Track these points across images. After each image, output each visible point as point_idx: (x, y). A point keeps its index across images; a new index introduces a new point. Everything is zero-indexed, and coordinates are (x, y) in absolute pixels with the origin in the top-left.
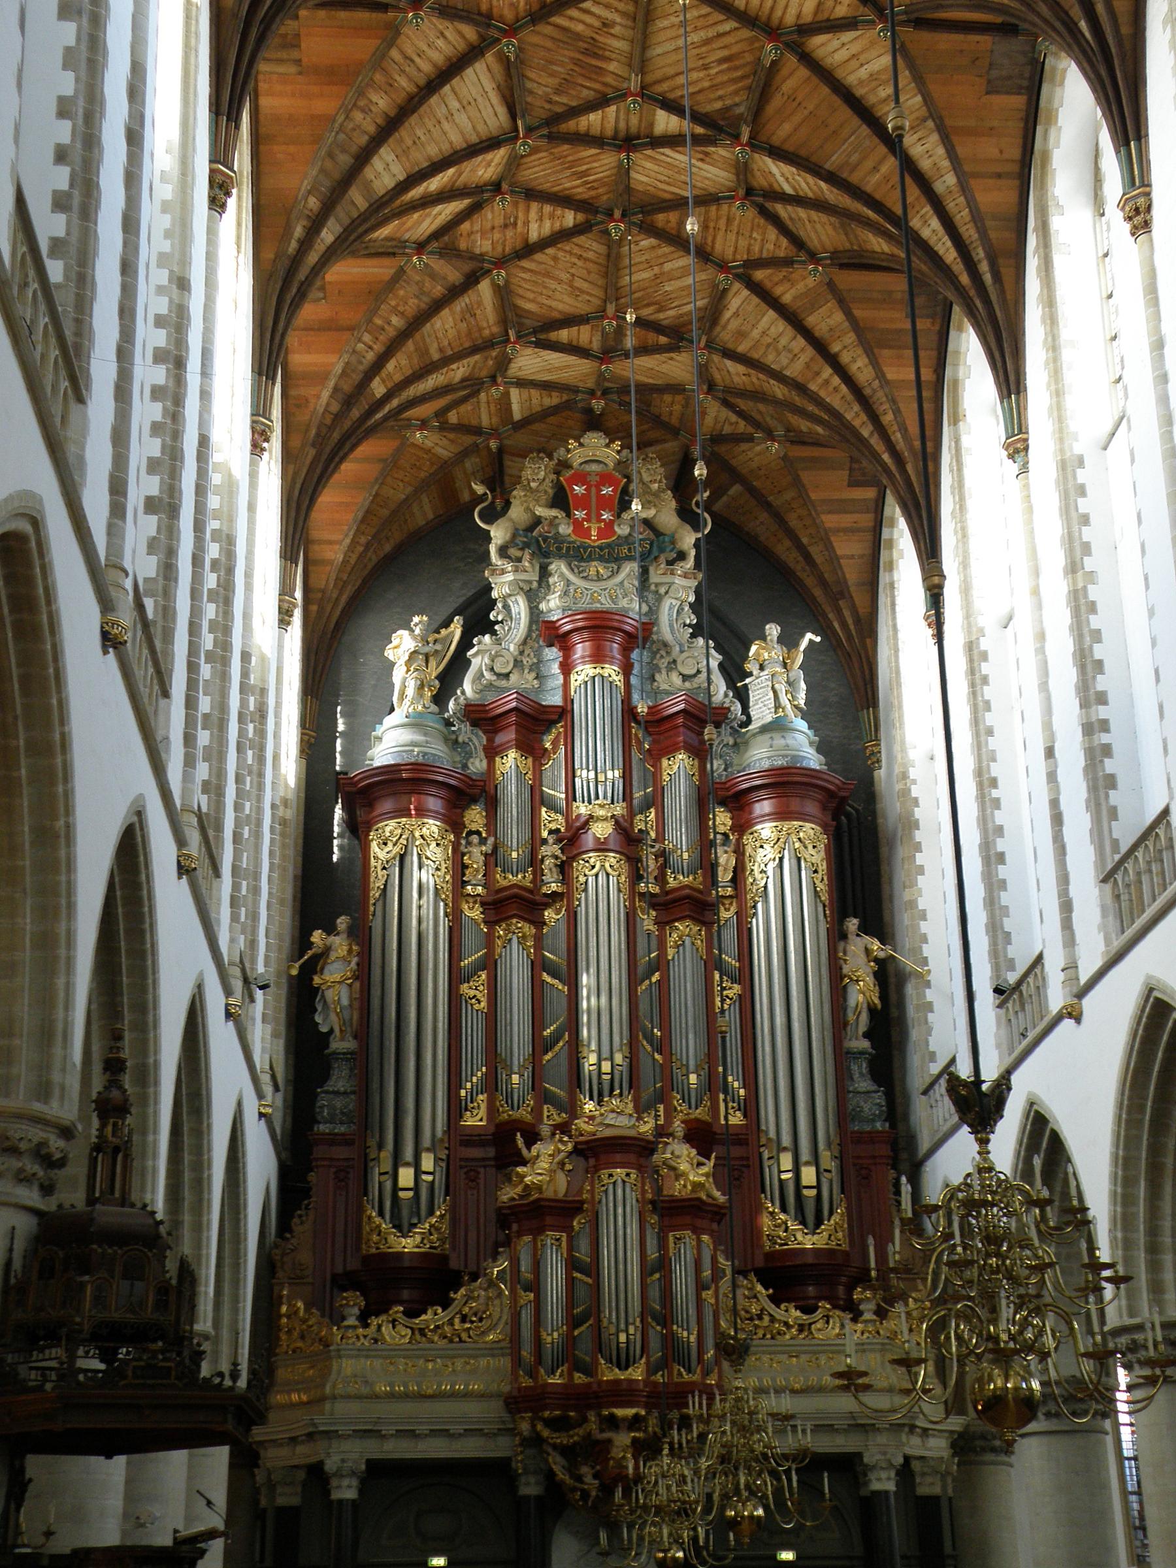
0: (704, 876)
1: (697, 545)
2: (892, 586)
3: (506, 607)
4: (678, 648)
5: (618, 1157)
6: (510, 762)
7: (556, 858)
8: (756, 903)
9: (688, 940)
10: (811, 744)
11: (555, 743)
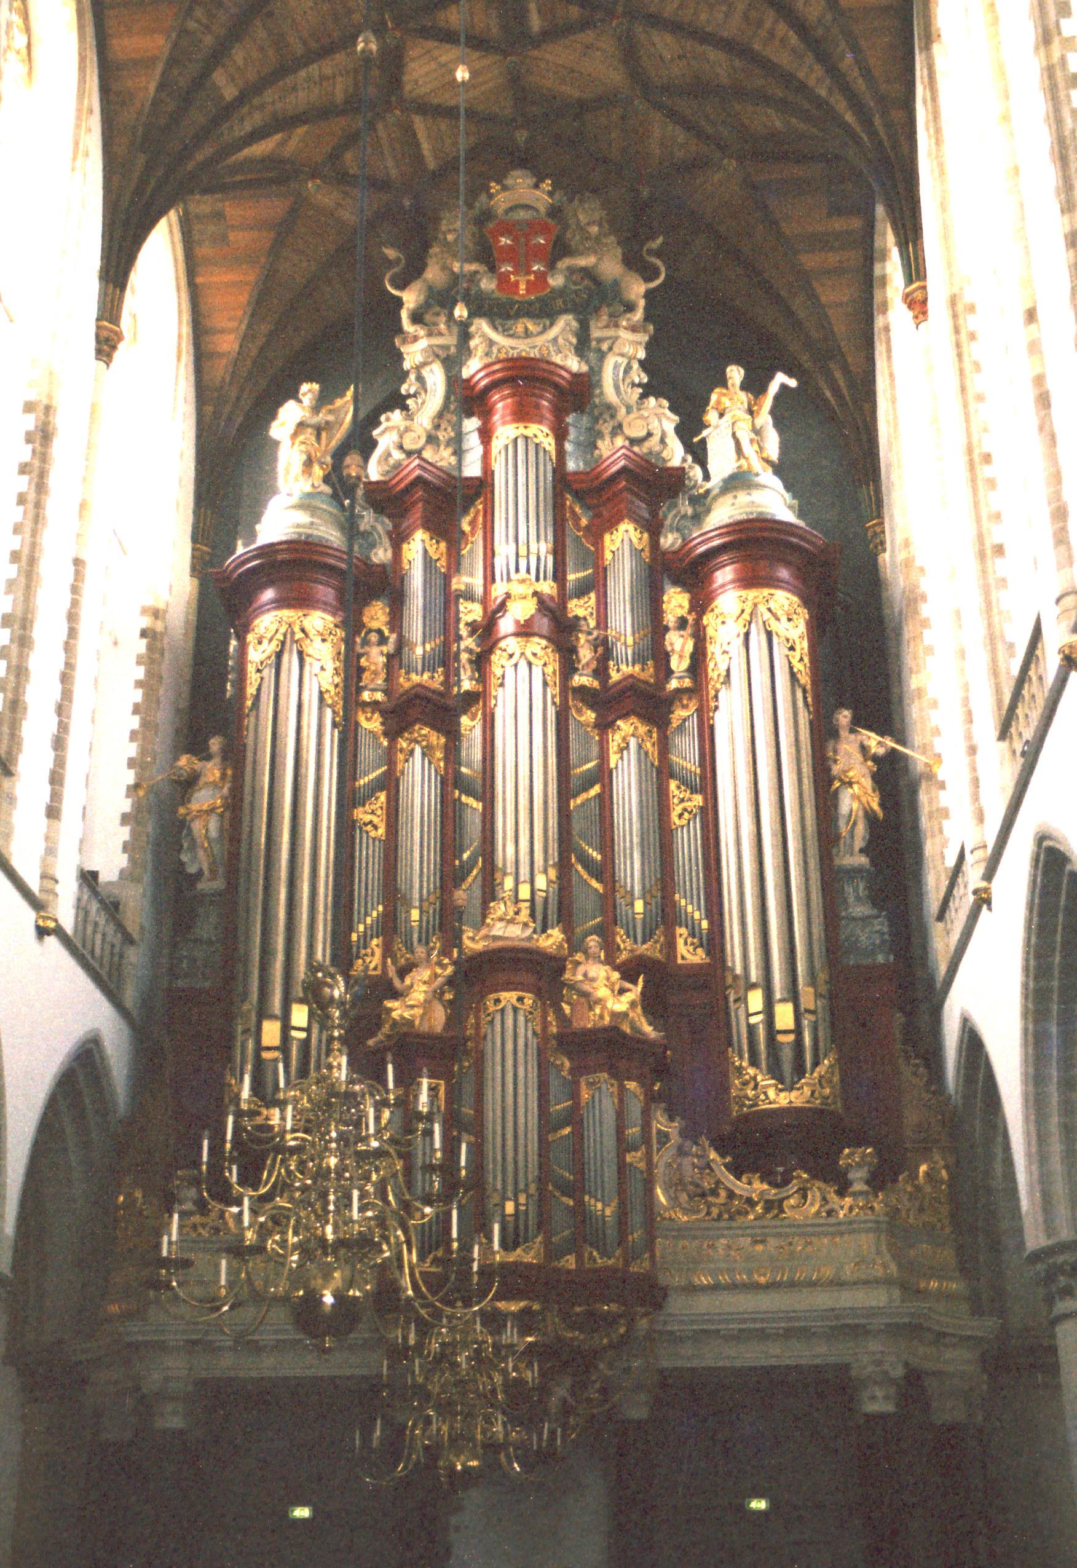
0: (656, 667)
1: (649, 295)
2: (887, 329)
3: (420, 379)
4: (623, 410)
5: (502, 977)
6: (418, 546)
7: (469, 651)
8: (717, 691)
9: (633, 742)
10: (790, 507)
11: (473, 523)
